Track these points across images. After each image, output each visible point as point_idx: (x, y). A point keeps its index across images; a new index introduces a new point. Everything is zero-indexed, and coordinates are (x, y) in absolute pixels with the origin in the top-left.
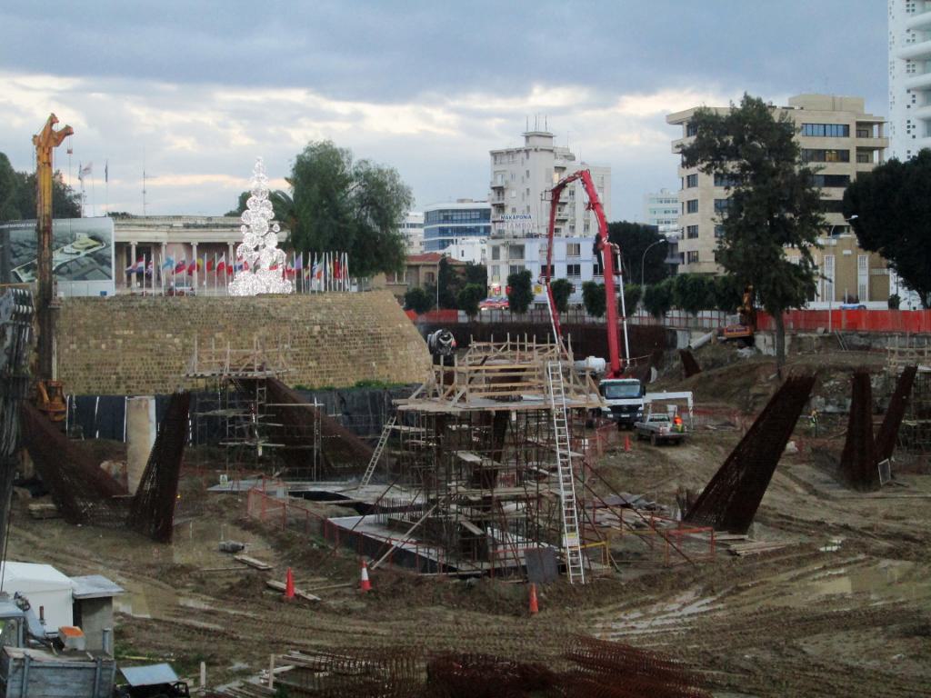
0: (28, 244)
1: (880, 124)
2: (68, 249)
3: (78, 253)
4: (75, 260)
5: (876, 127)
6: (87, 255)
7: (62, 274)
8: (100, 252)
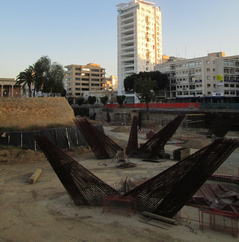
1: (104, 70)
5: (103, 70)
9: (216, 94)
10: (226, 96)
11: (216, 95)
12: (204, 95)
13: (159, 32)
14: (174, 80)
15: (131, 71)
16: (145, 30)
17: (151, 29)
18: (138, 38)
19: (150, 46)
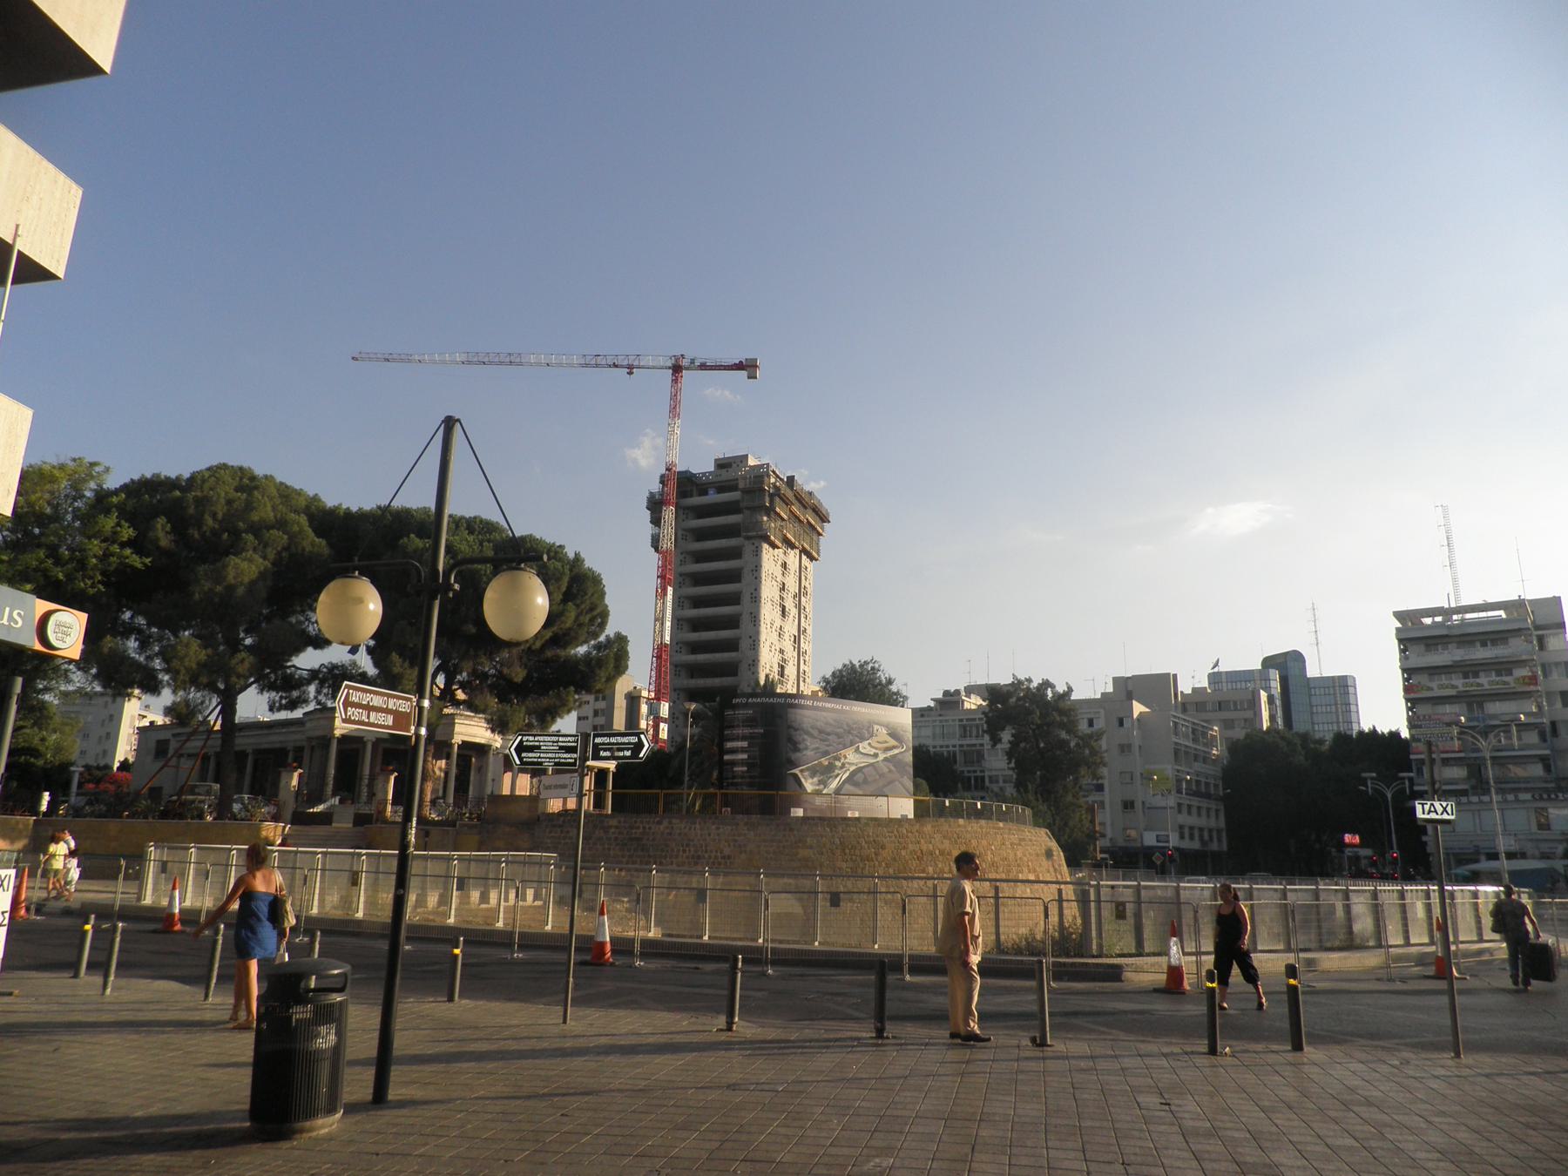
0: (815, 733)
2: (864, 747)
3: (876, 755)
4: (872, 764)
6: (886, 759)
7: (856, 784)
8: (900, 757)
9: (1157, 836)
10: (1187, 844)
11: (1158, 841)
12: (1111, 839)
13: (807, 585)
14: (976, 778)
15: (1318, 746)
16: (778, 570)
17: (792, 572)
18: (763, 601)
19: (786, 637)
